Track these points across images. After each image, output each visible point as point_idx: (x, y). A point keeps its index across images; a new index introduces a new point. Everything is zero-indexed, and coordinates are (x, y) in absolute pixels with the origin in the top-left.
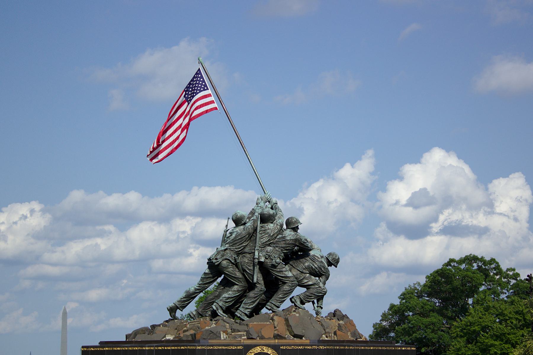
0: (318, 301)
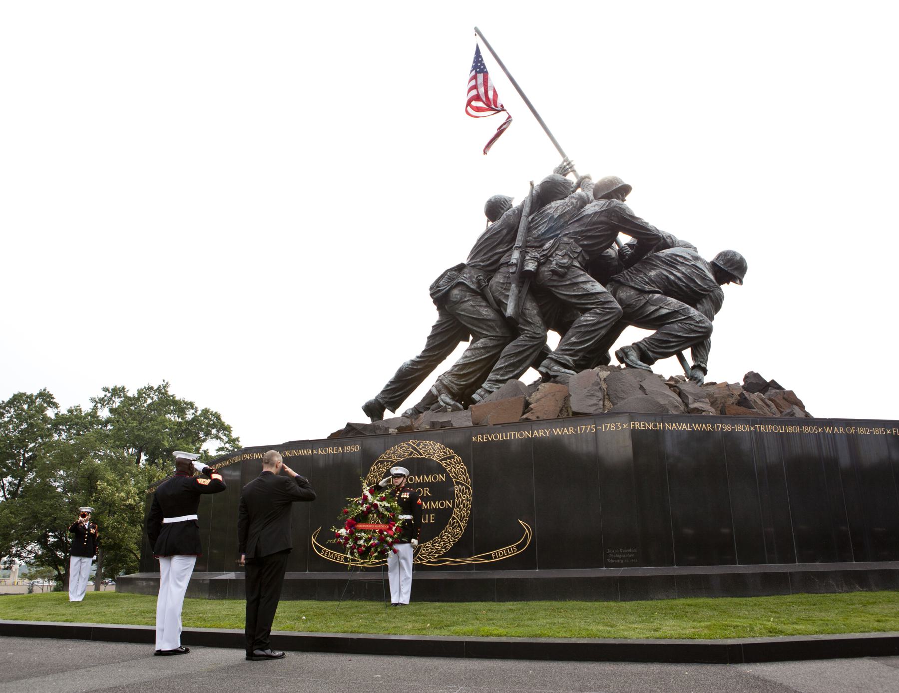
0: (694, 356)
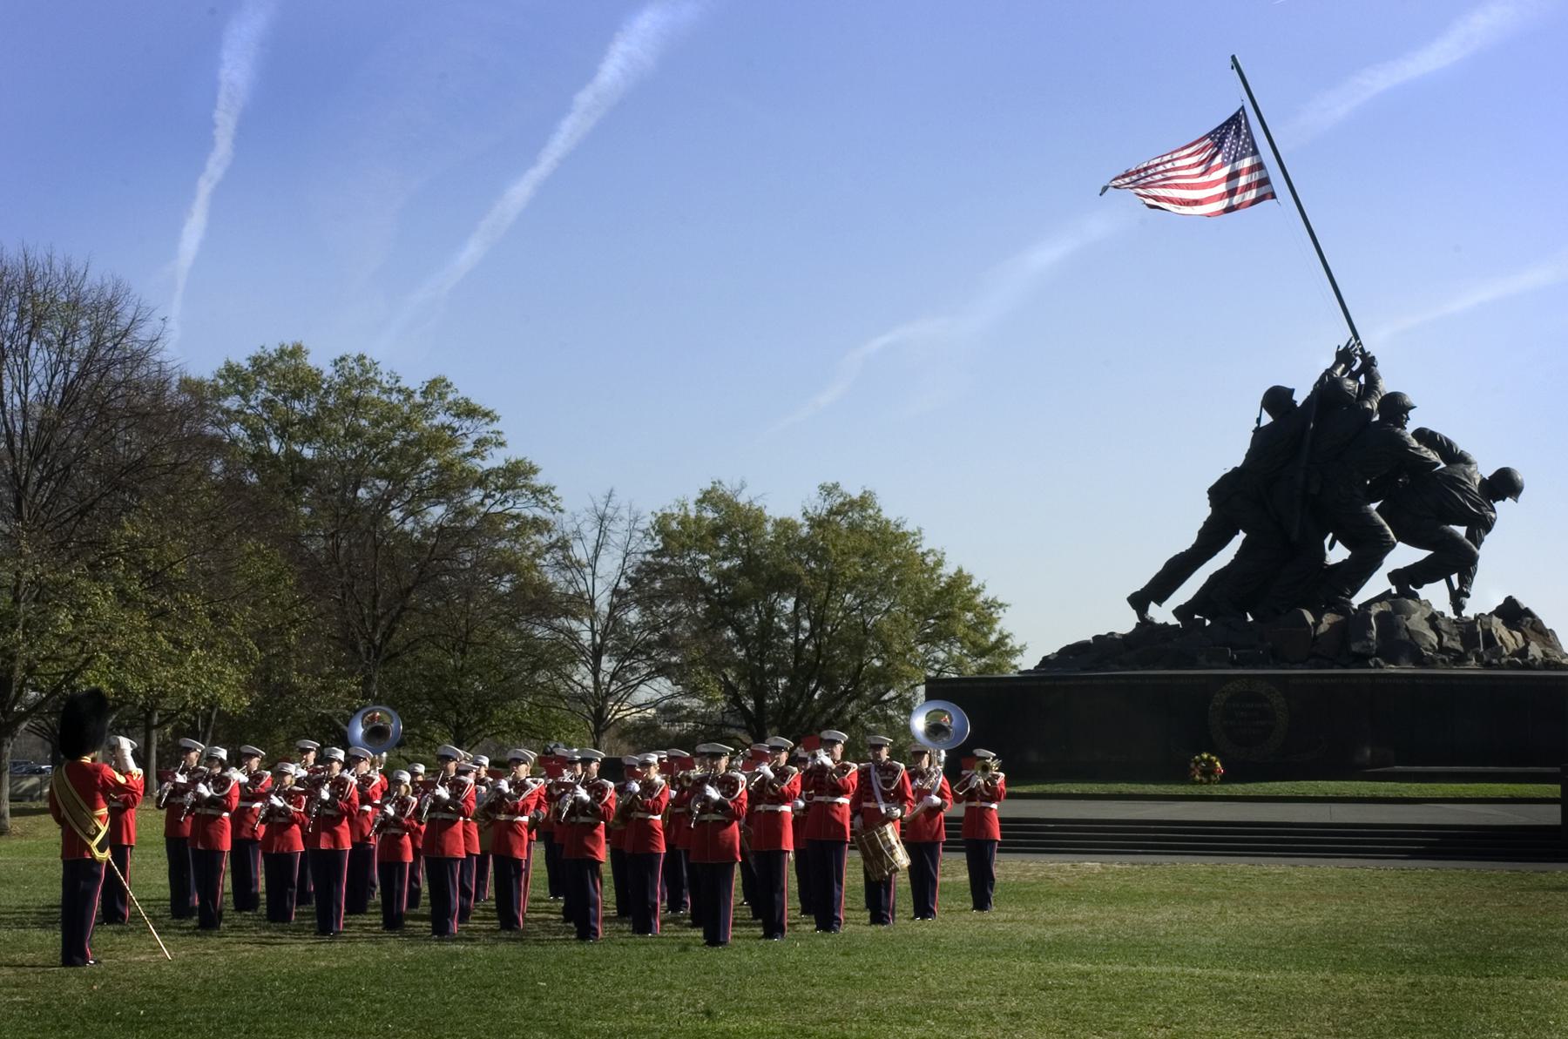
0: (1462, 581)
